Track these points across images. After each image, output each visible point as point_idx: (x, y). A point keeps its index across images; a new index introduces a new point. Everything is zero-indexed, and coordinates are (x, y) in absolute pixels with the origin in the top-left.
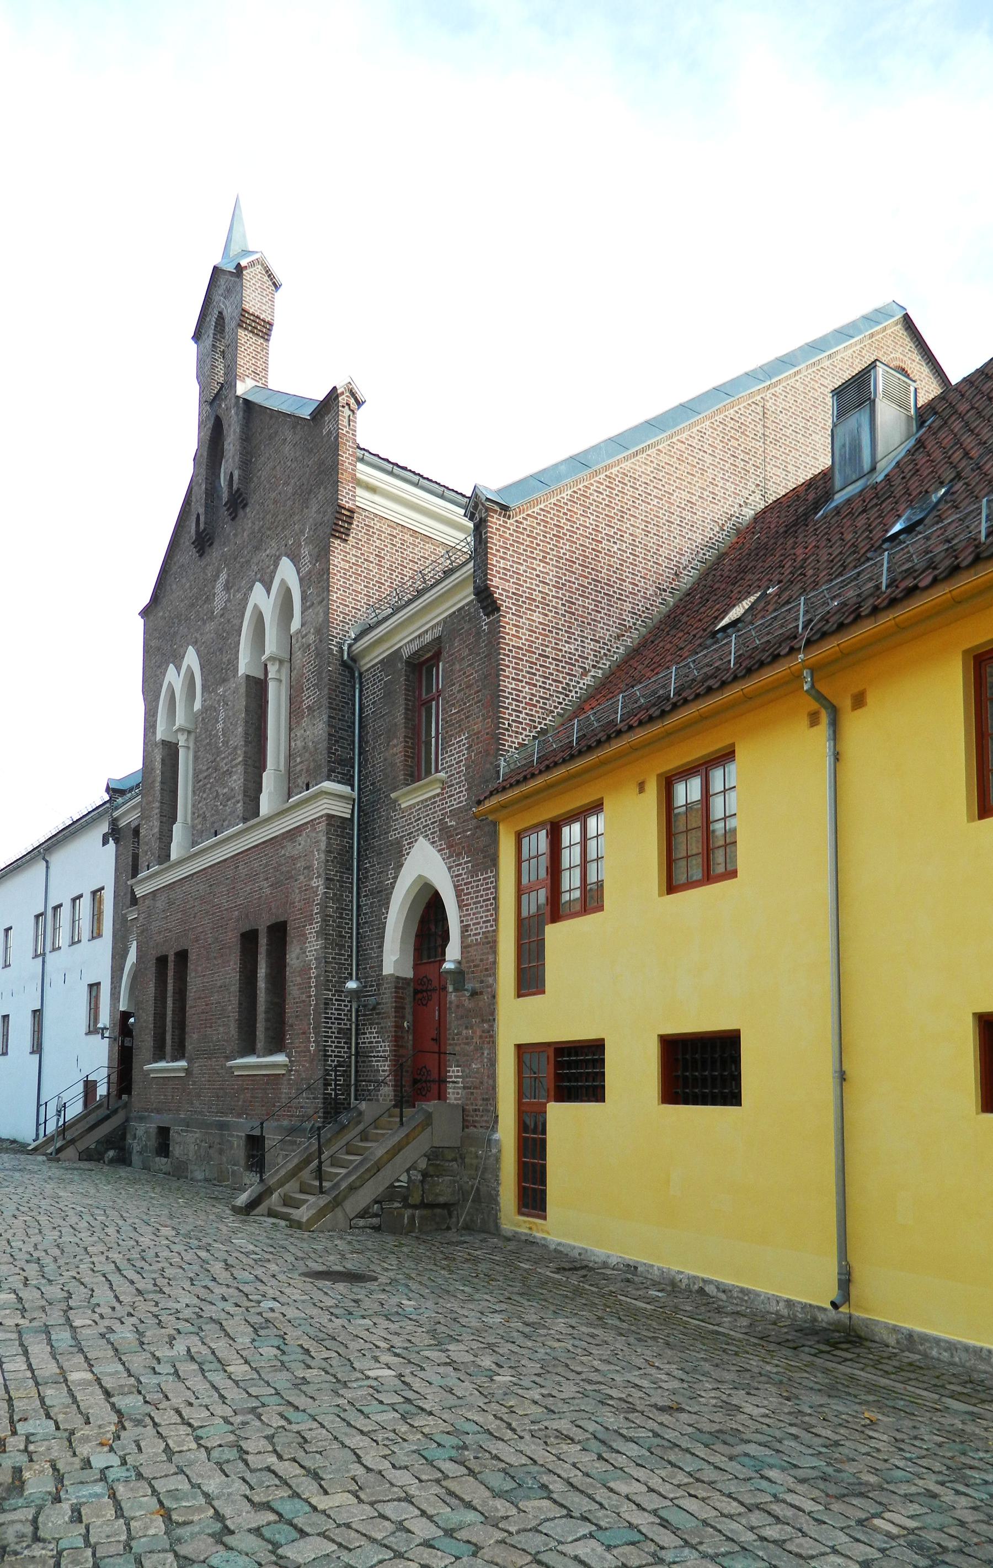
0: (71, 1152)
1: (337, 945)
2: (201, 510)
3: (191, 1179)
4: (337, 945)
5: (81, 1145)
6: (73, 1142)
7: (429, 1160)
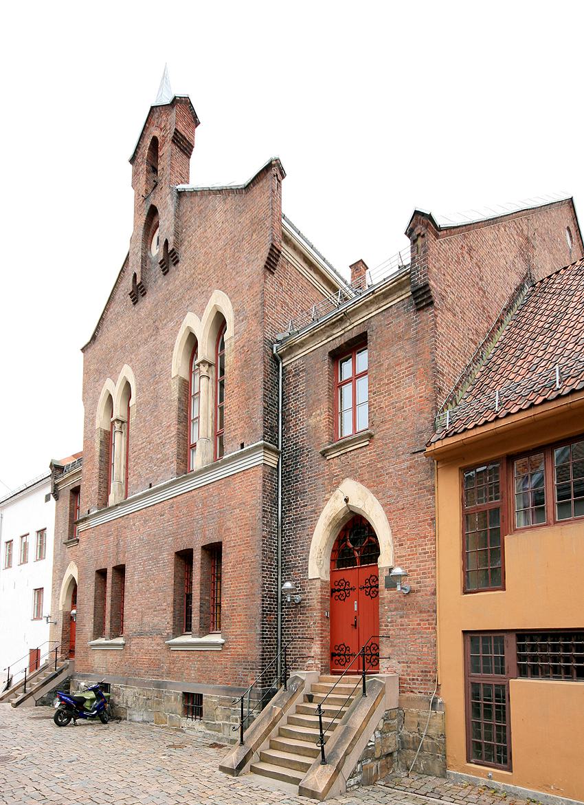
0: (31, 700)
1: (269, 558)
2: (138, 271)
3: (130, 720)
4: (269, 558)
5: (38, 696)
6: (31, 694)
7: (384, 720)
